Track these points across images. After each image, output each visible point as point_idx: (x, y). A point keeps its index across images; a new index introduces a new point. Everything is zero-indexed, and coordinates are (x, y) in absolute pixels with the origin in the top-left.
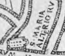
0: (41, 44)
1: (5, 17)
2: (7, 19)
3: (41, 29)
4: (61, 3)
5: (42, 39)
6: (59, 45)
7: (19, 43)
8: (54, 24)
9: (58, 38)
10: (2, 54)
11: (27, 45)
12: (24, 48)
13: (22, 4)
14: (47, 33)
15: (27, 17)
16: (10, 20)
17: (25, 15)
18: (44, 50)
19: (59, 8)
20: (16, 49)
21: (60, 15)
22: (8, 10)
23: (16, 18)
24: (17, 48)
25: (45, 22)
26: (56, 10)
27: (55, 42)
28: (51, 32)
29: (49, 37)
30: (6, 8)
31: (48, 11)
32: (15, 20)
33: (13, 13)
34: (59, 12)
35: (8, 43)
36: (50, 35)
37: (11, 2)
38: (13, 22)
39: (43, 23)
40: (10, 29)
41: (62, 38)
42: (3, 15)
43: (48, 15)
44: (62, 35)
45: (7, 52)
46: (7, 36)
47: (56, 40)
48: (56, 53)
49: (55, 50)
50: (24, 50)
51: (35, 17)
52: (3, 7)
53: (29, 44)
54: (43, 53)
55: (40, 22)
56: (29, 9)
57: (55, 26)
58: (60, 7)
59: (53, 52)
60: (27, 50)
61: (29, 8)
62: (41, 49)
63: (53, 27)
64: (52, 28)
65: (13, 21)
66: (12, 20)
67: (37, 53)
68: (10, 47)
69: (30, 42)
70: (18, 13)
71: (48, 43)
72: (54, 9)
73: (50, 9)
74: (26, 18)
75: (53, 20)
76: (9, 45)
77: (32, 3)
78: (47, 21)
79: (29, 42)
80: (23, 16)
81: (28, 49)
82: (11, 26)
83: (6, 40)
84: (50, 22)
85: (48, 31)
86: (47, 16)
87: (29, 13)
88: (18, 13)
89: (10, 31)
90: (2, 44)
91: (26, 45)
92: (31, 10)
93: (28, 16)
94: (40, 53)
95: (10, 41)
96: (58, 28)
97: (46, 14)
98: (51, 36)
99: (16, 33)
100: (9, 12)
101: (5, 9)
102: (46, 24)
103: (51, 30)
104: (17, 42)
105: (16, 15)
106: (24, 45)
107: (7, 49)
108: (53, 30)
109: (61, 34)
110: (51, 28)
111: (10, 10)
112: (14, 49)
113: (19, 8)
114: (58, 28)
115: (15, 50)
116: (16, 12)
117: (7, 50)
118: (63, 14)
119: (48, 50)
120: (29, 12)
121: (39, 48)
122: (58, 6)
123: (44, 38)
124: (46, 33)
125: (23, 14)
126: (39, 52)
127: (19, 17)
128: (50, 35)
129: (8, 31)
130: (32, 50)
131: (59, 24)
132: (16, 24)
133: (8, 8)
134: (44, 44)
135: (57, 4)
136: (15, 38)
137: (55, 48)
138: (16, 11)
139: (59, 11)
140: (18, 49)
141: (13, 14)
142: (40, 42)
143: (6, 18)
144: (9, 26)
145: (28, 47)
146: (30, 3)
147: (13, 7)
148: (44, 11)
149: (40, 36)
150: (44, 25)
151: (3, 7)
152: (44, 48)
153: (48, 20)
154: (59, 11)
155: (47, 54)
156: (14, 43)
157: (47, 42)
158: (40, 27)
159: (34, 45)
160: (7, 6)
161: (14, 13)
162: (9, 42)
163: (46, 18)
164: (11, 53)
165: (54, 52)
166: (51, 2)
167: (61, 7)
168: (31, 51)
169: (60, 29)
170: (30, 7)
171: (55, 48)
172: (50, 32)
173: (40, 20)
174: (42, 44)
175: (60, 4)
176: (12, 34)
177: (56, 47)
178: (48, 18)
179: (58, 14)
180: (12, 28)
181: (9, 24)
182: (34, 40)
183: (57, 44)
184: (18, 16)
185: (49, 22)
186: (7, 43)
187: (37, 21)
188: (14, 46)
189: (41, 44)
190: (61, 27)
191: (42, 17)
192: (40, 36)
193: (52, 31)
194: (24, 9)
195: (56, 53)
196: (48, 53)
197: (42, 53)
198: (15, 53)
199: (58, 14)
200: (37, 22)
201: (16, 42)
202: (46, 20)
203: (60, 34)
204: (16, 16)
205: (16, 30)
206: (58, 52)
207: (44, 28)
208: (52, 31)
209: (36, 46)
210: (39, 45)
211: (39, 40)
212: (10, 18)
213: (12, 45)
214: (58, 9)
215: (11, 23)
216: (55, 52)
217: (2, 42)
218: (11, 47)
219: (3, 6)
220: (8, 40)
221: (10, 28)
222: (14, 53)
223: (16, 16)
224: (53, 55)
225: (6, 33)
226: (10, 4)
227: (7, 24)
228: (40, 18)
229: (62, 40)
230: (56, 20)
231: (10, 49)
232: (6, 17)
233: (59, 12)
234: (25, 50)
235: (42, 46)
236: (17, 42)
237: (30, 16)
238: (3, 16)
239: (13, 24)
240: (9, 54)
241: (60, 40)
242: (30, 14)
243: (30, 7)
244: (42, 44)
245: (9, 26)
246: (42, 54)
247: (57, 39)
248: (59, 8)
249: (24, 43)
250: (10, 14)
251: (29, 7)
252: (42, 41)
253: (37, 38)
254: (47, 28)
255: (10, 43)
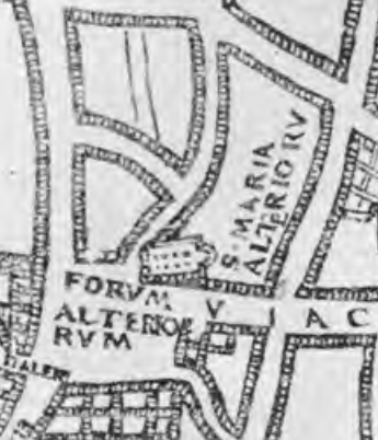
0: (259, 262)
1: (133, 166)
2: (139, 171)
3: (260, 208)
4: (332, 116)
5: (262, 242)
6: (326, 265)
7: (181, 260)
8: (304, 191)
9: (321, 242)
10: (124, 299)
11: (210, 265)
12: (200, 278)
13: (193, 119)
14: (283, 223)
15: (212, 164)
16: (150, 175)
17: (204, 160)
18: (270, 284)
19: (323, 134)
20: (173, 279)
21: (329, 159)
22: (145, 140)
23: (170, 170)
24: (176, 275)
25: (274, 182)
26: (314, 142)
27: (310, 255)
28: (297, 219)
29: (287, 236)
30: (138, 135)
31: (285, 146)
32: (168, 176)
33: (160, 151)
34: (323, 149)
35: (145, 257)
36: (292, 228)
37: (153, 114)
38: (161, 185)
39: (266, 188)
40: (150, 209)
41: (333, 240)
42: (125, 159)
43: (287, 158)
44: (335, 228)
45: (140, 290)
46: (139, 235)
47: (314, 246)
48: (314, 294)
49: (308, 282)
50: (199, 282)
51: (238, 164)
52: (124, 130)
53: (219, 260)
54: (268, 292)
55: (258, 183)
56: (218, 138)
57: (310, 198)
58: (327, 131)
59: (304, 292)
60: (211, 284)
61: (219, 135)
62: (260, 280)
63: (303, 202)
64: (299, 204)
65: (161, 179)
66: (158, 176)
67: (247, 292)
68: (149, 271)
69: (221, 254)
70: (180, 152)
71: (284, 258)
72: (305, 136)
73: (293, 138)
74: (206, 170)
75: (303, 176)
76: (145, 263)
77: (227, 117)
78: (280, 179)
79: (216, 256)
80: (196, 164)
81: (216, 281)
82: (153, 199)
83: (137, 248)
84: (291, 185)
85: (287, 215)
86: (280, 163)
87: (218, 150)
88: (180, 152)
89: (150, 215)
90: (121, 260)
91: (206, 264)
92: (225, 141)
93: (216, 161)
94: (255, 294)
95: (152, 251)
96: (321, 207)
97: (276, 155)
98: (294, 233)
99: (172, 222)
100: (147, 147)
101: (131, 137)
102: (278, 191)
103: (295, 213)
104: (175, 255)
105: (170, 158)
106: (201, 265)
107: (141, 281)
108: (304, 211)
109: (332, 225)
110: (295, 203)
111: (151, 140)
112: (164, 279)
113: (183, 134)
114: (321, 207)
115: (167, 283)
116: (171, 148)
117: (139, 284)
118: (339, 155)
119: (284, 282)
120: (218, 146)
121: (254, 275)
122: (322, 127)
123: (270, 241)
124: (278, 222)
125: (195, 155)
126: (252, 292)
127: (182, 166)
128: (292, 228)
129: (144, 215)
130: (228, 283)
131: (322, 191)
132: (173, 191)
133: (143, 134)
134: (272, 261)
135: (318, 121)
136: (169, 239)
137: (310, 276)
138: (172, 145)
139: (325, 142)
140: (180, 278)
141: (160, 156)
142: (256, 255)
143: (135, 170)
144: (146, 198)
145: (216, 271)
146: (222, 116)
147: (161, 130)
148: (272, 145)
149: (258, 232)
150: (271, 196)
151: (124, 130)
152: (271, 275)
153: (284, 176)
154: (325, 143)
155: (280, 298)
156: (165, 257)
157: (282, 255)
158: (256, 200)
159: (234, 266)
160: (139, 126)
161: (163, 153)
162: (148, 255)
163: (276, 169)
164: (154, 294)
165: (307, 289)
166: (294, 113)
167: (331, 129)
168: (224, 286)
169: (329, 208)
170: (221, 129)
171: (310, 276)
172: (293, 218)
173: (257, 175)
174: (263, 261)
175: (328, 119)
176: (156, 226)
177: (312, 273)
178: (284, 169)
179: (320, 155)
180: (157, 203)
181: (145, 191)
182: (235, 247)
183: (317, 260)
184: (180, 163)
185: (287, 184)
186: (141, 257)
187: (248, 180)
188: (166, 267)
189: (259, 262)
190: (331, 200)
191: (264, 165)
192: (258, 232)
193: (297, 216)
194: (200, 137)
195: (314, 294)
196: (283, 294)
197: (262, 295)
198: (169, 295)
199: (320, 155)
200: (247, 184)
201: (171, 256)
202: (276, 178)
203: (327, 228)
204: (173, 160)
205: (171, 211)
206: (320, 290)
207: (270, 206)
208: (297, 216)
209: (242, 268)
210: (253, 266)
211: (253, 247)
212: (150, 169)
213: (157, 266)
214: (320, 139)
215: (154, 186)
216: (309, 291)
217: (123, 253)
218: (155, 271)
219: (127, 126)
220: (144, 249)
221: (149, 204)
222: (165, 295)
223: (173, 160)
224: (301, 300)
225: (135, 221)
226: (149, 120)
227: (140, 191)
228: (256, 167)
229: (333, 246)
230: (313, 174)
231: (151, 279)
232: (138, 165)
233: (323, 149)
234: (203, 282)
235: (264, 268)
236: (175, 255)
237: (220, 163)
238: (127, 163)
239: (161, 192)
240: (146, 298)
241: (328, 246)
242: (220, 153)
243: (221, 129)
244: (263, 261)
245: (146, 198)
246: (265, 296)
247: (317, 242)
248: (323, 134)
249: (201, 256)
250: (151, 156)
251: (217, 130)
252: (263, 249)
253: (245, 239)
254: (281, 203)
255: (151, 258)
